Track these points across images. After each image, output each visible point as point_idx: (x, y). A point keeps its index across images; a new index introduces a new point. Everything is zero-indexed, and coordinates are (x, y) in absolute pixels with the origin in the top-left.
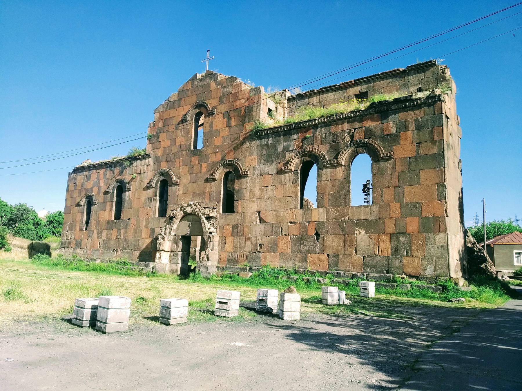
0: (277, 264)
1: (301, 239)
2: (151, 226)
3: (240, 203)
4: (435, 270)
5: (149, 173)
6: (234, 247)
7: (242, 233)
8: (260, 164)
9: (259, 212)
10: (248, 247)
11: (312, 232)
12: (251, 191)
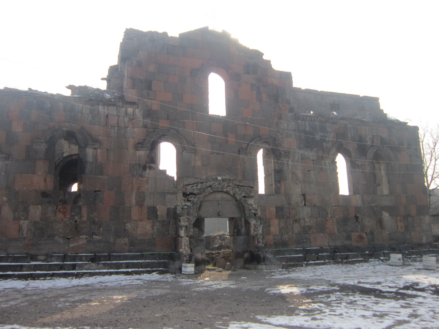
0: (327, 243)
1: (345, 221)
2: (149, 202)
3: (282, 184)
4: (427, 240)
5: (136, 130)
6: (280, 230)
7: (288, 215)
8: (300, 148)
9: (304, 195)
10: (297, 228)
11: (352, 215)
12: (293, 173)
